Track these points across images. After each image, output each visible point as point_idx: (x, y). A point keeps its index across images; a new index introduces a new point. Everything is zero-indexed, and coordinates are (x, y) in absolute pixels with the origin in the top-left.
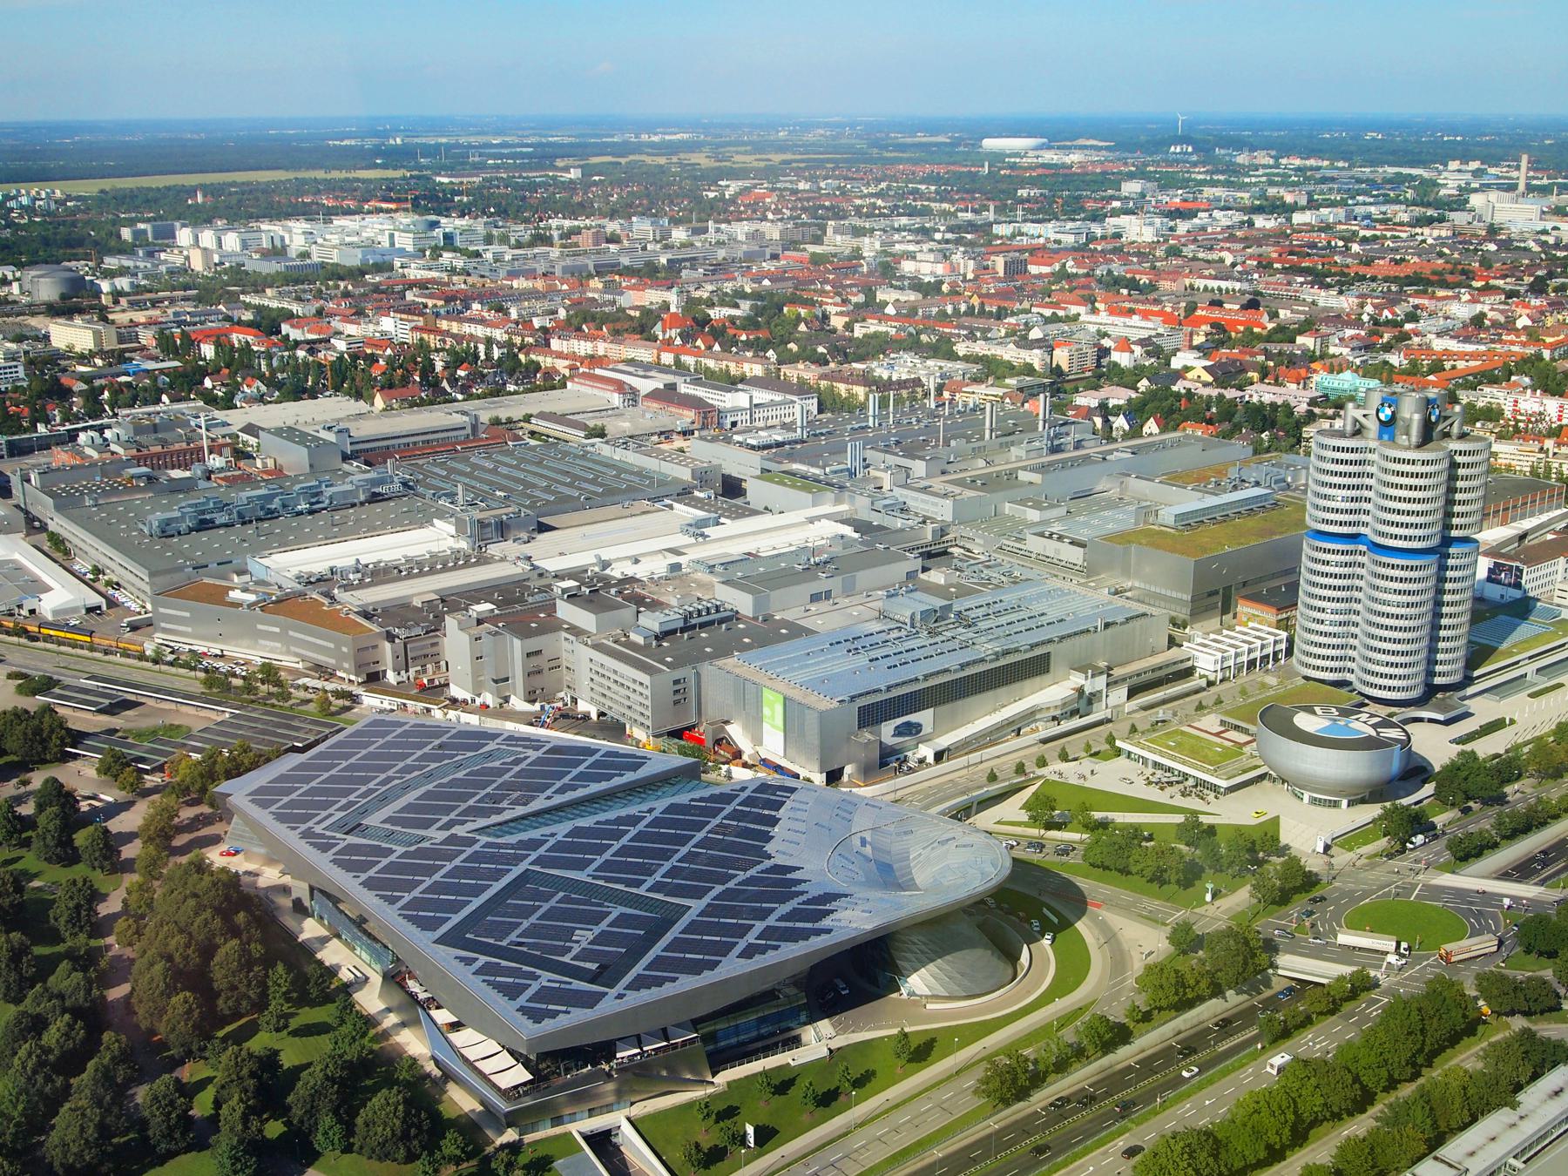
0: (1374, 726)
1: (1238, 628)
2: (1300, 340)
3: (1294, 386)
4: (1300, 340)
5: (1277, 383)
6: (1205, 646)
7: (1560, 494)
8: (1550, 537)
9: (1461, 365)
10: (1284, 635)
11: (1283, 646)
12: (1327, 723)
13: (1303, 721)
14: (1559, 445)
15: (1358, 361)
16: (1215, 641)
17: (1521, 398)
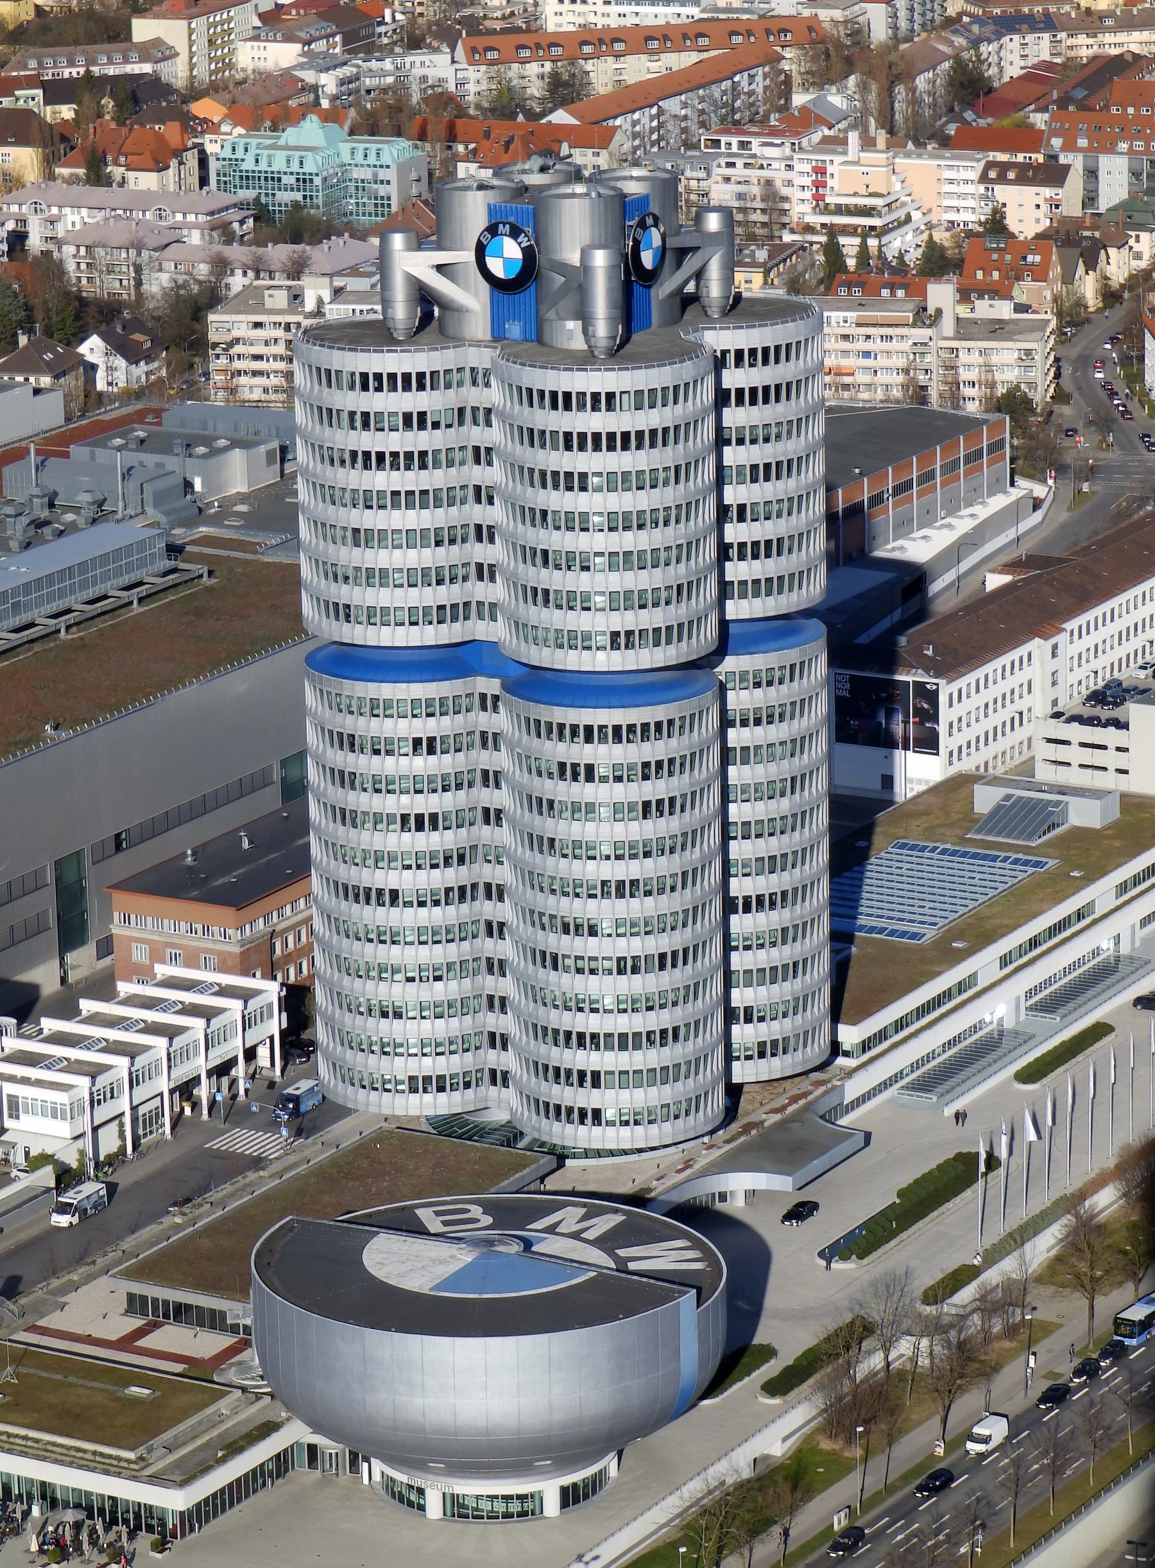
0: (606, 1242)
1: (124, 988)
2: (143, 29)
3: (146, 181)
4: (143, 29)
5: (97, 177)
6: (32, 1060)
7: (996, 447)
8: (995, 581)
9: (639, 69)
10: (272, 990)
11: (275, 1025)
12: (464, 1256)
13: (392, 1260)
14: (965, 295)
15: (329, 82)
16: (58, 1039)
17: (835, 165)
